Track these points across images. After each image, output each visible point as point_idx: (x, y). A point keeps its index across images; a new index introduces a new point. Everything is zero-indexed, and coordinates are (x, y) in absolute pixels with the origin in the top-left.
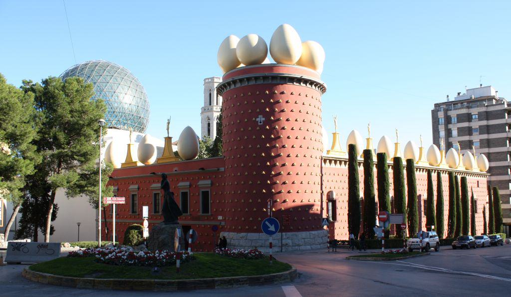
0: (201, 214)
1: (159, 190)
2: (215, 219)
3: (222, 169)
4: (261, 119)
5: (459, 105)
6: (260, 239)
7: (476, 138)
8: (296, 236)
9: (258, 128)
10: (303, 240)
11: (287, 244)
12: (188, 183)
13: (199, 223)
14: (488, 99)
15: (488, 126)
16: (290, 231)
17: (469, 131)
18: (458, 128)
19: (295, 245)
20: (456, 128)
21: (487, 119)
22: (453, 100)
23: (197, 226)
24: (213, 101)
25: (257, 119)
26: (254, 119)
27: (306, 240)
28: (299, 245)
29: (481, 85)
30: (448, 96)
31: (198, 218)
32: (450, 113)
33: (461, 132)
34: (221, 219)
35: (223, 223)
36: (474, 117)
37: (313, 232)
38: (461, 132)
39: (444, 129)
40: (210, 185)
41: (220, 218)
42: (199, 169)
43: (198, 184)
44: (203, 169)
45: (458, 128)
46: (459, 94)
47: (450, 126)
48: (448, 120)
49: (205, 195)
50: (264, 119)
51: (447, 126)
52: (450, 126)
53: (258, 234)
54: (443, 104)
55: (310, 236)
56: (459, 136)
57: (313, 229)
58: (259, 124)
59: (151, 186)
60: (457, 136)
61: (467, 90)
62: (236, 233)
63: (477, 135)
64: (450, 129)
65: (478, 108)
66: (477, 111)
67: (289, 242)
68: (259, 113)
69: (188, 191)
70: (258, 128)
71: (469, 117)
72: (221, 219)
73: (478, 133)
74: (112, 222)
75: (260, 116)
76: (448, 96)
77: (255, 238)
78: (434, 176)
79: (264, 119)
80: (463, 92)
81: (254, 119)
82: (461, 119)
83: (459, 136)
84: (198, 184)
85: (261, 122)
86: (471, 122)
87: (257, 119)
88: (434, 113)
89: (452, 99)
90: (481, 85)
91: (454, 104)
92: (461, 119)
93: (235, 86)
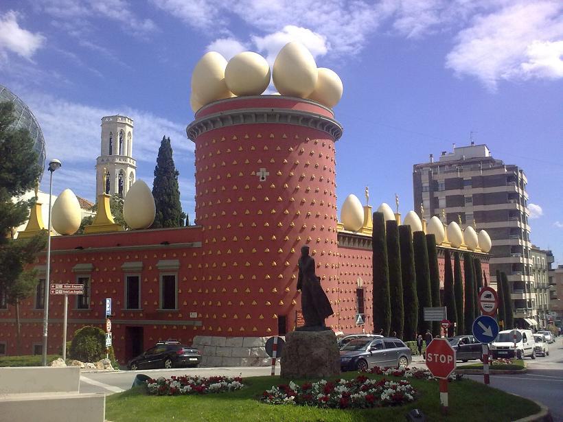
0: (161, 308)
1: (88, 273)
3: (198, 244)
4: (263, 173)
5: (447, 167)
7: (469, 209)
9: (260, 187)
12: (140, 264)
13: (156, 323)
17: (460, 201)
18: (447, 197)
21: (484, 187)
23: (155, 327)
24: (116, 149)
25: (258, 174)
26: (253, 173)
29: (473, 143)
30: (431, 156)
31: (156, 316)
32: (436, 177)
33: (451, 201)
34: (196, 316)
35: (199, 323)
39: (429, 198)
41: (194, 315)
42: (162, 244)
45: (447, 197)
46: (444, 153)
47: (436, 194)
48: (434, 186)
49: (169, 282)
50: (268, 174)
51: (433, 194)
52: (436, 194)
54: (427, 165)
56: (447, 206)
58: (261, 180)
62: (225, 338)
65: (472, 172)
68: (261, 165)
69: (140, 276)
70: (260, 187)
71: (460, 184)
72: (196, 316)
73: (471, 204)
74: (62, 324)
75: (261, 169)
76: (431, 156)
79: (268, 174)
80: (450, 150)
81: (253, 173)
82: (451, 184)
83: (447, 206)
85: (263, 178)
87: (258, 174)
90: (473, 143)
91: (440, 166)
92: (451, 184)
93: (223, 125)
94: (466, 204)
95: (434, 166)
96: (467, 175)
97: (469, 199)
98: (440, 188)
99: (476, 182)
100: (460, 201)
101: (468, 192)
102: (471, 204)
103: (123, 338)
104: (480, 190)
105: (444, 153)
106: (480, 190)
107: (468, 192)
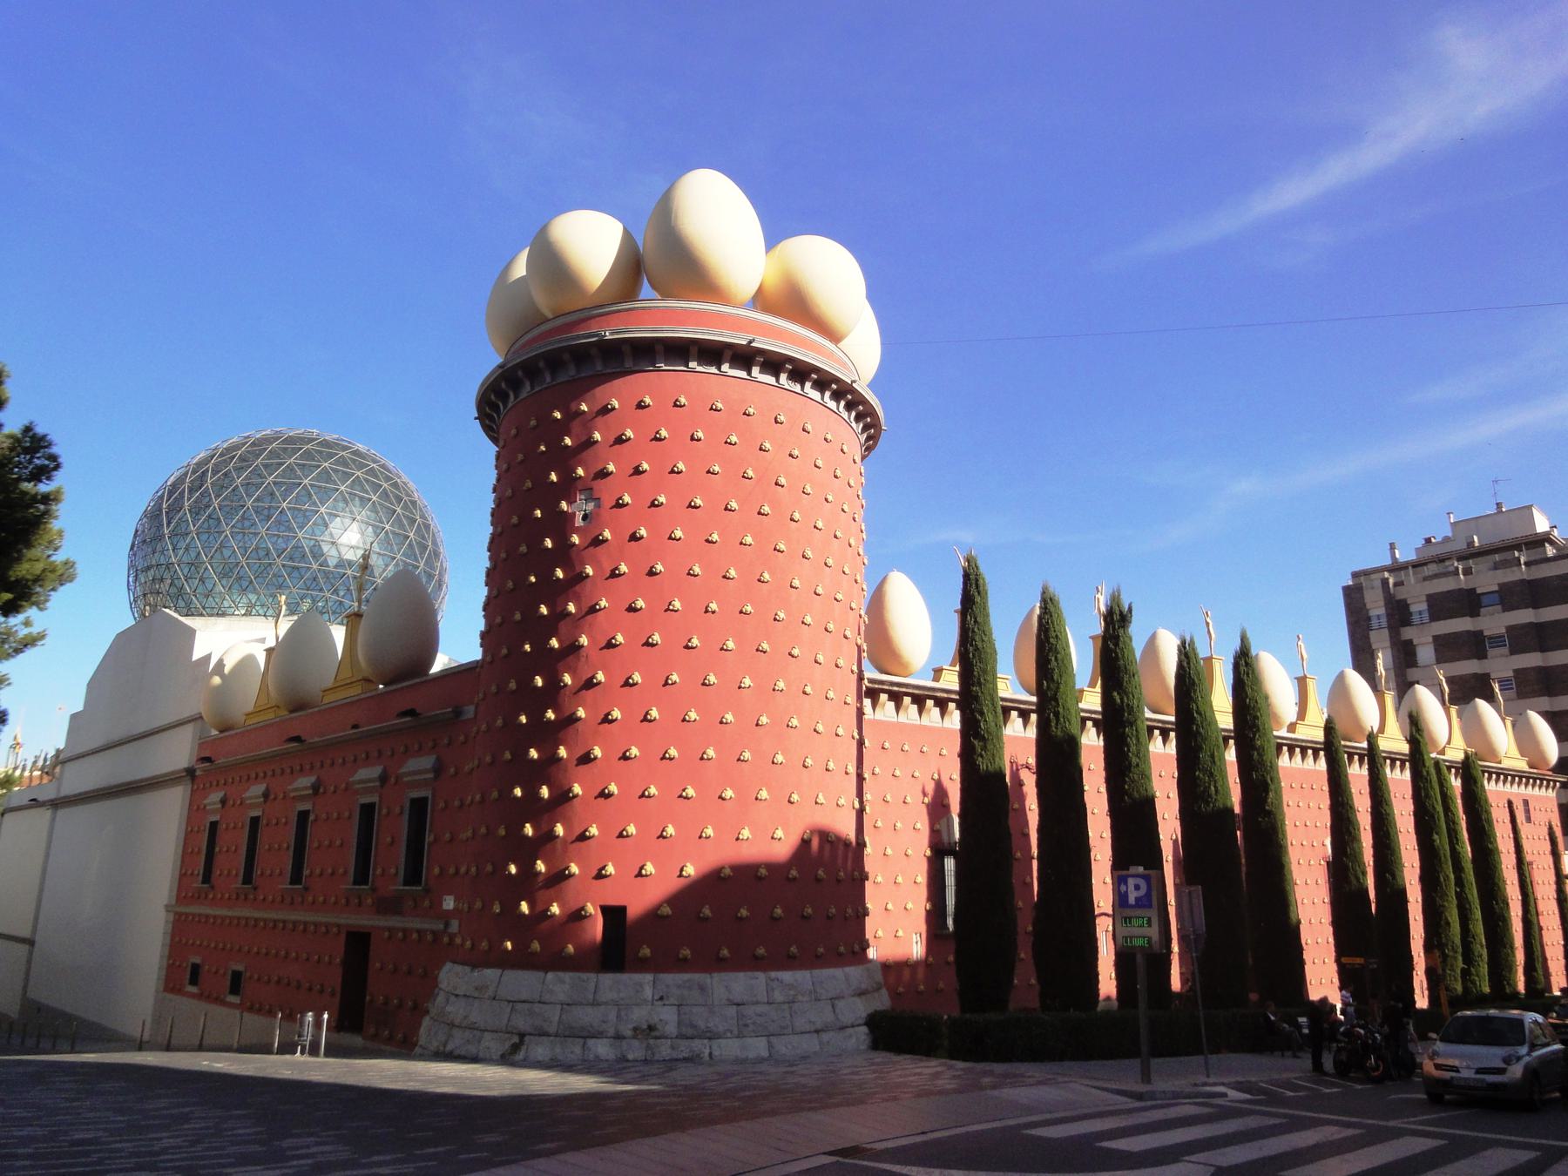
2: (435, 911)
6: (547, 997)
7: (1501, 665)
8: (702, 988)
10: (732, 1010)
11: (651, 1028)
14: (1526, 544)
15: (1539, 628)
16: (681, 965)
17: (1476, 645)
18: (1436, 639)
19: (690, 1032)
20: (1431, 639)
22: (1411, 556)
27: (750, 1011)
28: (711, 1036)
29: (1499, 505)
36: (1485, 600)
37: (787, 976)
38: (1447, 648)
40: (431, 776)
43: (403, 770)
44: (411, 713)
45: (1436, 639)
46: (1428, 541)
47: (1408, 633)
48: (1399, 613)
49: (419, 806)
52: (1408, 633)
53: (541, 974)
55: (769, 990)
57: (790, 963)
59: (295, 785)
60: (1433, 659)
61: (1454, 525)
63: (1502, 656)
64: (1410, 642)
66: (1497, 582)
67: (667, 1017)
71: (1469, 602)
73: (1505, 650)
77: (524, 996)
78: (1357, 774)
80: (1440, 532)
84: (403, 770)
86: (1478, 615)
88: (1353, 597)
89: (1405, 554)
90: (1499, 505)
91: (1414, 566)
92: (1441, 606)
94: (1491, 652)
95: (1396, 568)
96: (1487, 580)
97: (1497, 641)
98: (1416, 618)
99: (1510, 597)
100: (1476, 645)
101: (1494, 622)
102: (1505, 650)
103: (338, 960)
104: (1525, 616)
105: (1428, 541)
106: (1525, 616)
107: (1494, 622)
